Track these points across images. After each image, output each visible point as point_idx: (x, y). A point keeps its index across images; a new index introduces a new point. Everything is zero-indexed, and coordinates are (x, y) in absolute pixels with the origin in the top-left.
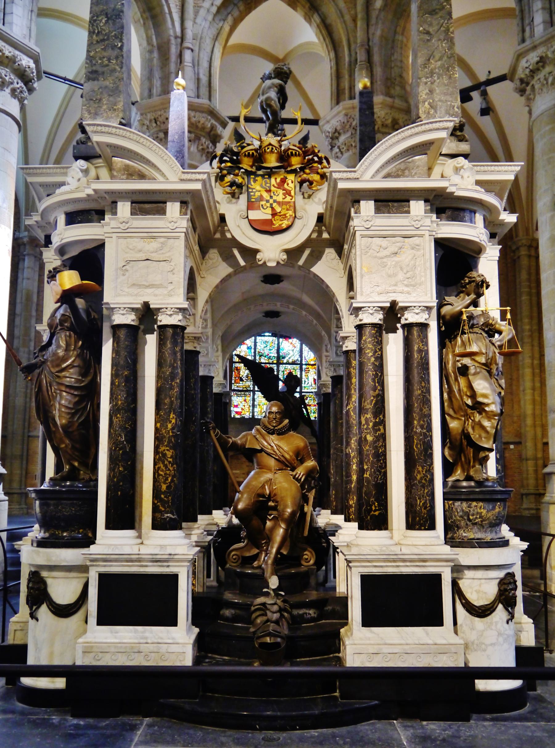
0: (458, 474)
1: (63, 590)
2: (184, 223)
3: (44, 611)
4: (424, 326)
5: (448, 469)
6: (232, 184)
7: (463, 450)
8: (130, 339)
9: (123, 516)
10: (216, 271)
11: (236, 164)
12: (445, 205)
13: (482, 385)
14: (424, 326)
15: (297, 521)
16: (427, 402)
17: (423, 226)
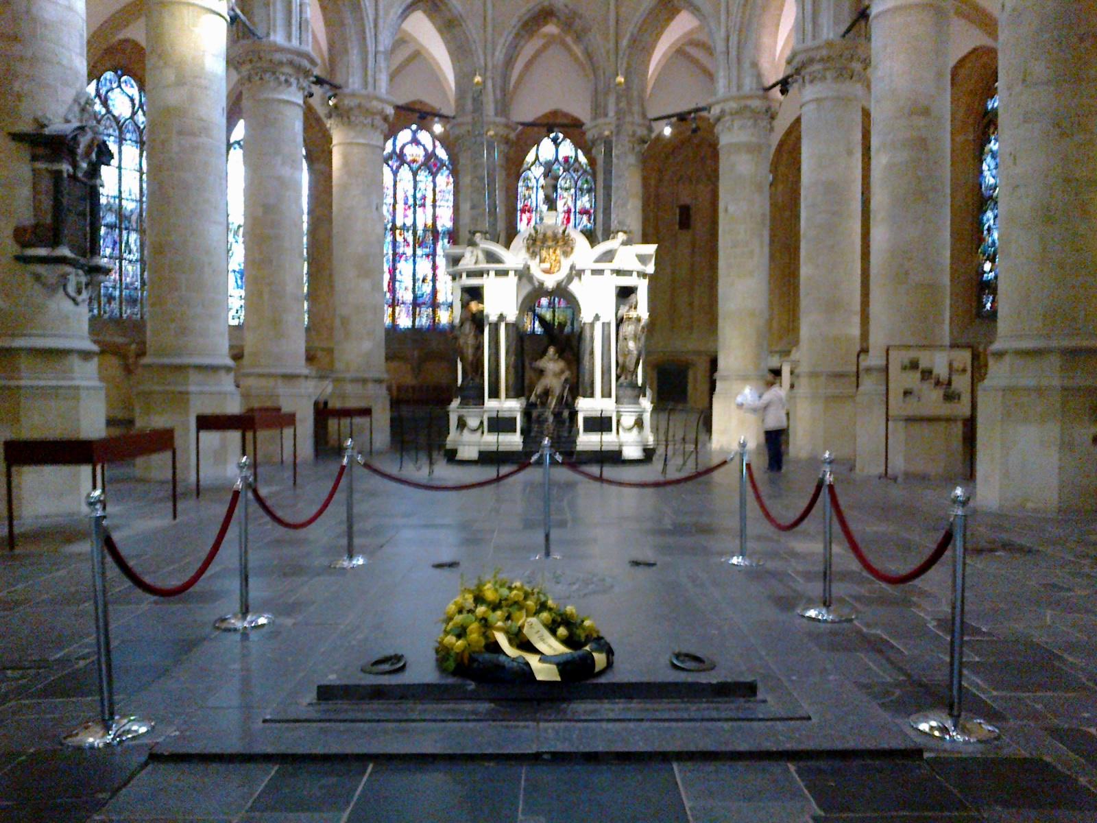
0: (622, 378)
1: (473, 422)
2: (516, 279)
3: (465, 431)
4: (609, 324)
5: (618, 377)
6: (533, 252)
7: (622, 369)
8: (495, 328)
9: (495, 394)
10: (527, 289)
11: (535, 241)
12: (618, 272)
13: (632, 345)
14: (609, 324)
15: (561, 398)
16: (609, 350)
17: (612, 283)
